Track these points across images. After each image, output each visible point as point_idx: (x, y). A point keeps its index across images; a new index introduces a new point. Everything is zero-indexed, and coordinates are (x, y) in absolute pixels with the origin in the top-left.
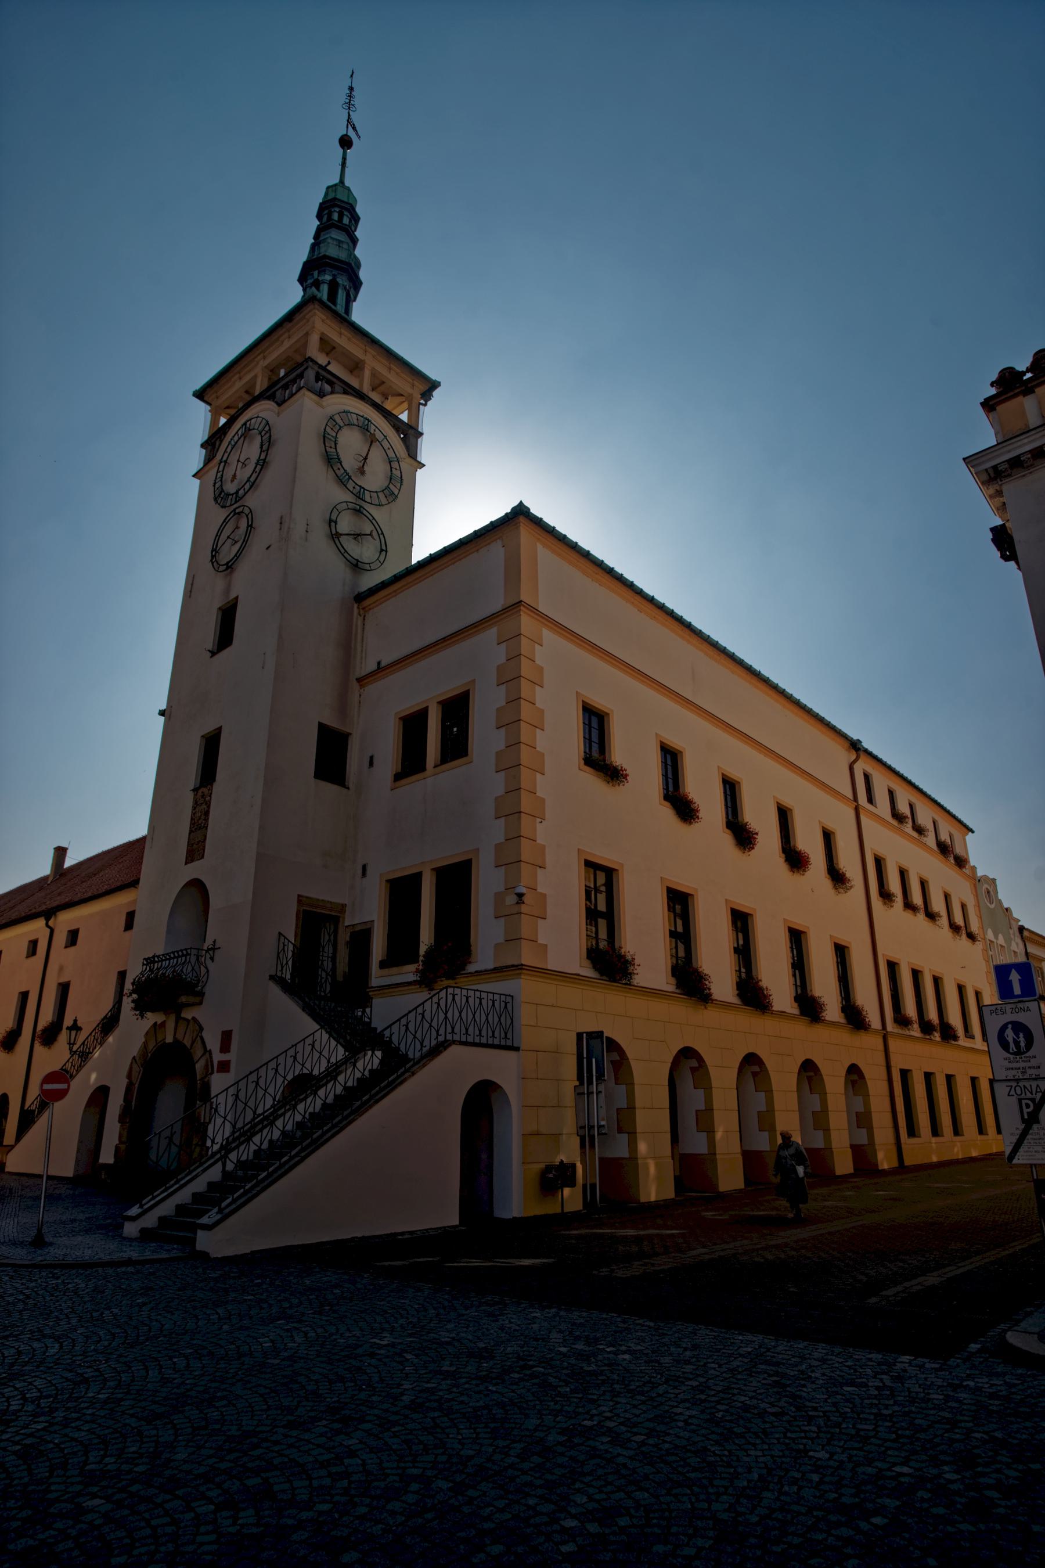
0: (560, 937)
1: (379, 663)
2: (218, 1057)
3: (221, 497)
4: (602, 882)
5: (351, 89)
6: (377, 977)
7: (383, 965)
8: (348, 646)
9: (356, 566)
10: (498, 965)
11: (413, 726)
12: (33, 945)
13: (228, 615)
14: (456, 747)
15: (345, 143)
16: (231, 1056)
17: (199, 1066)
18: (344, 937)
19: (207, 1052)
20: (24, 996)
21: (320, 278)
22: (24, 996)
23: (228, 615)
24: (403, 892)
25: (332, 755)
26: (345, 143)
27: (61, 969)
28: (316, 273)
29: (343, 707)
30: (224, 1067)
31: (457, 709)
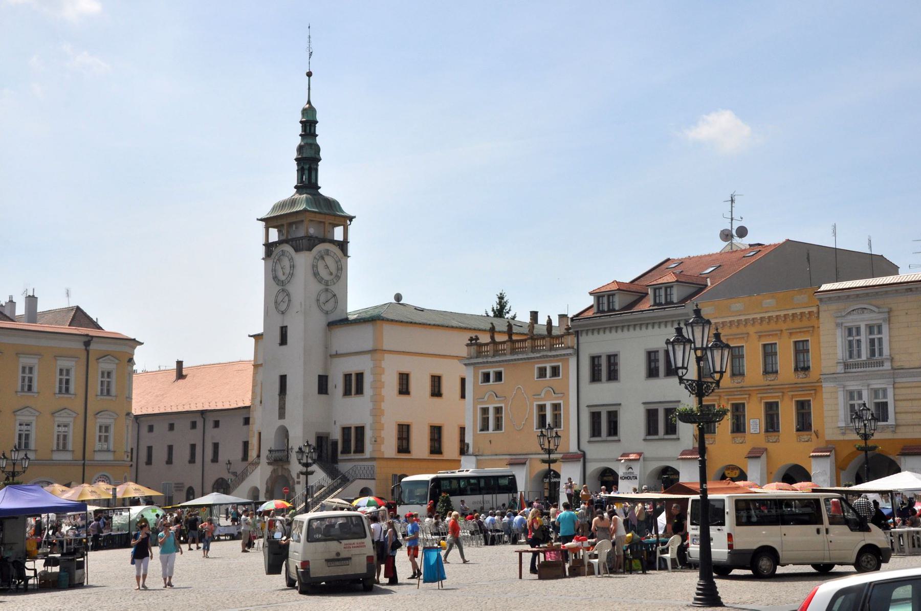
0: (389, 447)
2: (296, 480)
3: (275, 278)
4: (404, 432)
6: (340, 456)
7: (342, 453)
8: (326, 347)
9: (327, 313)
11: (347, 377)
12: (194, 425)
13: (284, 331)
14: (360, 391)
15: (309, 74)
17: (291, 482)
18: (329, 443)
19: (293, 479)
20: (193, 447)
22: (193, 447)
23: (284, 331)
24: (346, 431)
25: (323, 385)
26: (309, 74)
29: (326, 366)
31: (360, 376)
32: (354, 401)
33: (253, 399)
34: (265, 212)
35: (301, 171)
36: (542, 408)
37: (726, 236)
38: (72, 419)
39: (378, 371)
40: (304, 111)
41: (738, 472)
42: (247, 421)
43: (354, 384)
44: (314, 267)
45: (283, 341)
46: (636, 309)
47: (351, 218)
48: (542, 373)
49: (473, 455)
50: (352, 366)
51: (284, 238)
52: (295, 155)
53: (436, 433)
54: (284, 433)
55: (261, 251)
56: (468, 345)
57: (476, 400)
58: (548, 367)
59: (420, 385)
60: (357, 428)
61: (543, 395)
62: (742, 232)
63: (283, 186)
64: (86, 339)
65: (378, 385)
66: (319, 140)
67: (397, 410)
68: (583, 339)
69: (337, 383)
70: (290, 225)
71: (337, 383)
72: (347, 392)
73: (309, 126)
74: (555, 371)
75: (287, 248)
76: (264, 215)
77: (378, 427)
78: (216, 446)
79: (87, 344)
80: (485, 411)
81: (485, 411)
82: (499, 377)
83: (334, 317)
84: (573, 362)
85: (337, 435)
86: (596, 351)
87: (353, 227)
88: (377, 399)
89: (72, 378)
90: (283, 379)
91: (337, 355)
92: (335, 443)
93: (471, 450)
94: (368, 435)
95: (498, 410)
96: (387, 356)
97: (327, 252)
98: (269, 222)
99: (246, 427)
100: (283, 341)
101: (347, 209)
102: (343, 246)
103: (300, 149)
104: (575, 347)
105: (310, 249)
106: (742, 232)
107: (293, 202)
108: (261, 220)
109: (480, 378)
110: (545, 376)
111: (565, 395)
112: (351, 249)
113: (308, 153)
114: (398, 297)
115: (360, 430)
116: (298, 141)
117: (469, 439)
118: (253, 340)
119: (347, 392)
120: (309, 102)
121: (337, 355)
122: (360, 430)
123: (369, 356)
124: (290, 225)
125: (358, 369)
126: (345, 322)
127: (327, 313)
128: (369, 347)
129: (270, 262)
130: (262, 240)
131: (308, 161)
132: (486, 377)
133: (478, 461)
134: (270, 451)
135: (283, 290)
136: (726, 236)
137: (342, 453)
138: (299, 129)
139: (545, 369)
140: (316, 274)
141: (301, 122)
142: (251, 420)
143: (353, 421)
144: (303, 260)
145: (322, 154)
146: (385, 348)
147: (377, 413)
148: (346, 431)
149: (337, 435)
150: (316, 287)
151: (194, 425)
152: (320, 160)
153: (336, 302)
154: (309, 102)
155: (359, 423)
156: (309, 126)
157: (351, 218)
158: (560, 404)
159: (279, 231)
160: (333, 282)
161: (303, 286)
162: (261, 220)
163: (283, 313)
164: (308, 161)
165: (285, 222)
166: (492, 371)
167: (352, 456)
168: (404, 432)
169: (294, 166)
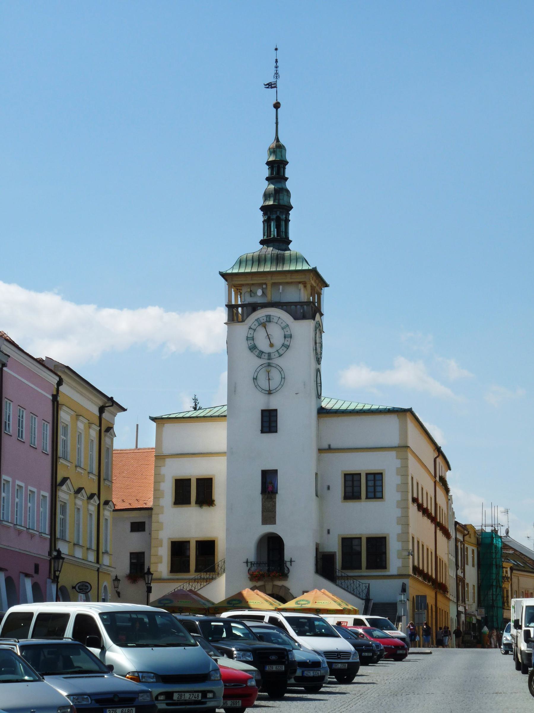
1: (329, 446)
5: (276, 61)
10: (399, 573)
15: (277, 106)
21: (281, 217)
26: (277, 106)
28: (278, 213)
63: (248, 236)
73: (277, 169)
85: (334, 546)
94: (394, 548)
107: (260, 260)
116: (266, 186)
120: (277, 140)
124: (274, 284)
130: (225, 302)
131: (277, 213)
135: (269, 365)
138: (266, 172)
140: (253, 348)
141: (268, 163)
149: (334, 546)
154: (277, 140)
156: (277, 169)
164: (277, 213)
165: (269, 280)
167: (364, 572)
169: (260, 217)
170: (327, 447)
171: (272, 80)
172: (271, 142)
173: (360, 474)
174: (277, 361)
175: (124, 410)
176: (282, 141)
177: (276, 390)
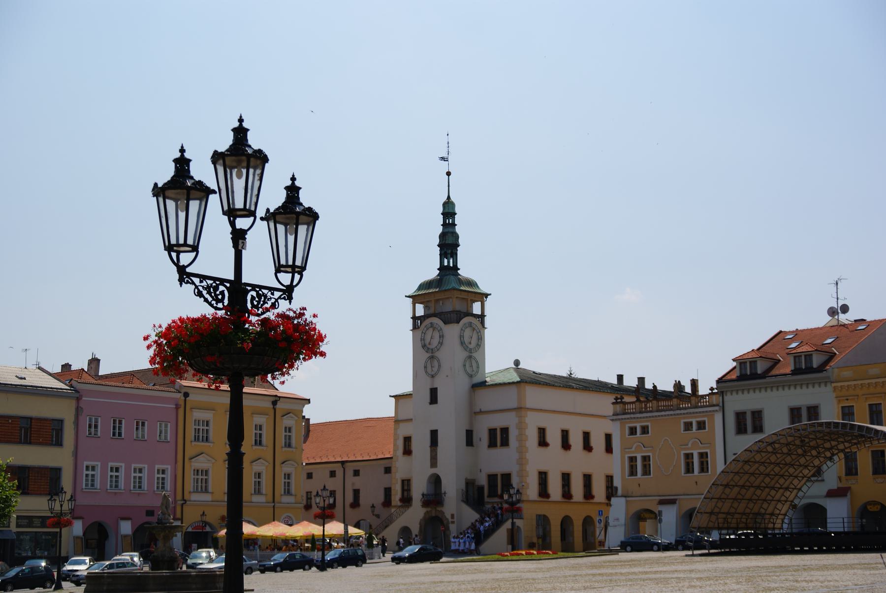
0: (532, 491)
2: (450, 520)
3: (424, 346)
4: (543, 477)
6: (486, 499)
7: (489, 496)
8: (471, 403)
11: (492, 432)
12: (333, 474)
13: (434, 393)
14: (505, 443)
15: (448, 174)
16: (455, 520)
17: (445, 522)
19: (447, 519)
23: (434, 393)
26: (448, 174)
27: (353, 484)
30: (453, 522)
31: (505, 431)
32: (499, 451)
33: (395, 450)
34: (412, 289)
35: (443, 255)
36: (689, 456)
37: (832, 312)
38: (264, 468)
39: (521, 426)
40: (445, 204)
41: (879, 507)
42: (388, 470)
43: (499, 438)
44: (461, 337)
45: (434, 399)
46: (774, 372)
47: (487, 295)
48: (688, 426)
49: (622, 496)
50: (497, 422)
51: (432, 311)
52: (437, 241)
53: (566, 478)
54: (436, 481)
55: (410, 324)
56: (613, 403)
57: (624, 449)
58: (638, 426)
59: (554, 438)
60: (502, 475)
61: (690, 445)
62: (845, 309)
64: (273, 399)
65: (522, 438)
66: (458, 229)
67: (538, 459)
68: (728, 398)
69: (482, 436)
70: (437, 301)
71: (482, 436)
72: (492, 444)
74: (701, 425)
75: (436, 321)
76: (410, 293)
77: (522, 474)
78: (356, 493)
79: (274, 403)
80: (633, 460)
81: (633, 460)
82: (645, 430)
83: (477, 379)
84: (718, 418)
85: (483, 481)
86: (740, 408)
87: (488, 302)
88: (522, 450)
89: (264, 432)
90: (434, 434)
91: (481, 412)
92: (481, 489)
93: (620, 492)
94: (515, 481)
95: (646, 459)
96: (529, 413)
97: (470, 324)
98: (416, 299)
99: (387, 475)
100: (434, 399)
101: (483, 288)
102: (482, 317)
103: (442, 236)
104: (721, 404)
105: (458, 322)
106: (845, 309)
108: (409, 297)
109: (627, 431)
110: (636, 434)
111: (712, 444)
112: (488, 321)
113: (450, 240)
114: (517, 363)
115: (507, 477)
116: (440, 229)
117: (617, 482)
118: (393, 399)
119: (492, 444)
120: (449, 197)
121: (481, 412)
122: (507, 477)
123: (513, 414)
125: (503, 424)
126: (483, 384)
127: (471, 376)
128: (514, 405)
129: (419, 332)
132: (633, 431)
133: (627, 501)
134: (423, 495)
136: (832, 312)
137: (489, 496)
139: (691, 423)
142: (393, 470)
143: (499, 469)
144: (452, 331)
145: (460, 241)
146: (528, 406)
147: (522, 462)
148: (492, 478)
149: (483, 481)
150: (461, 355)
151: (333, 474)
152: (459, 246)
153: (478, 367)
154: (449, 197)
155: (506, 470)
157: (487, 295)
158: (649, 457)
159: (425, 308)
160: (473, 349)
161: (452, 354)
162: (409, 297)
163: (433, 376)
166: (638, 426)
168: (543, 477)
170: (478, 410)
171: (445, 155)
172: (445, 199)
173: (496, 429)
174: (437, 354)
175: (308, 401)
176: (453, 199)
177: (436, 374)
